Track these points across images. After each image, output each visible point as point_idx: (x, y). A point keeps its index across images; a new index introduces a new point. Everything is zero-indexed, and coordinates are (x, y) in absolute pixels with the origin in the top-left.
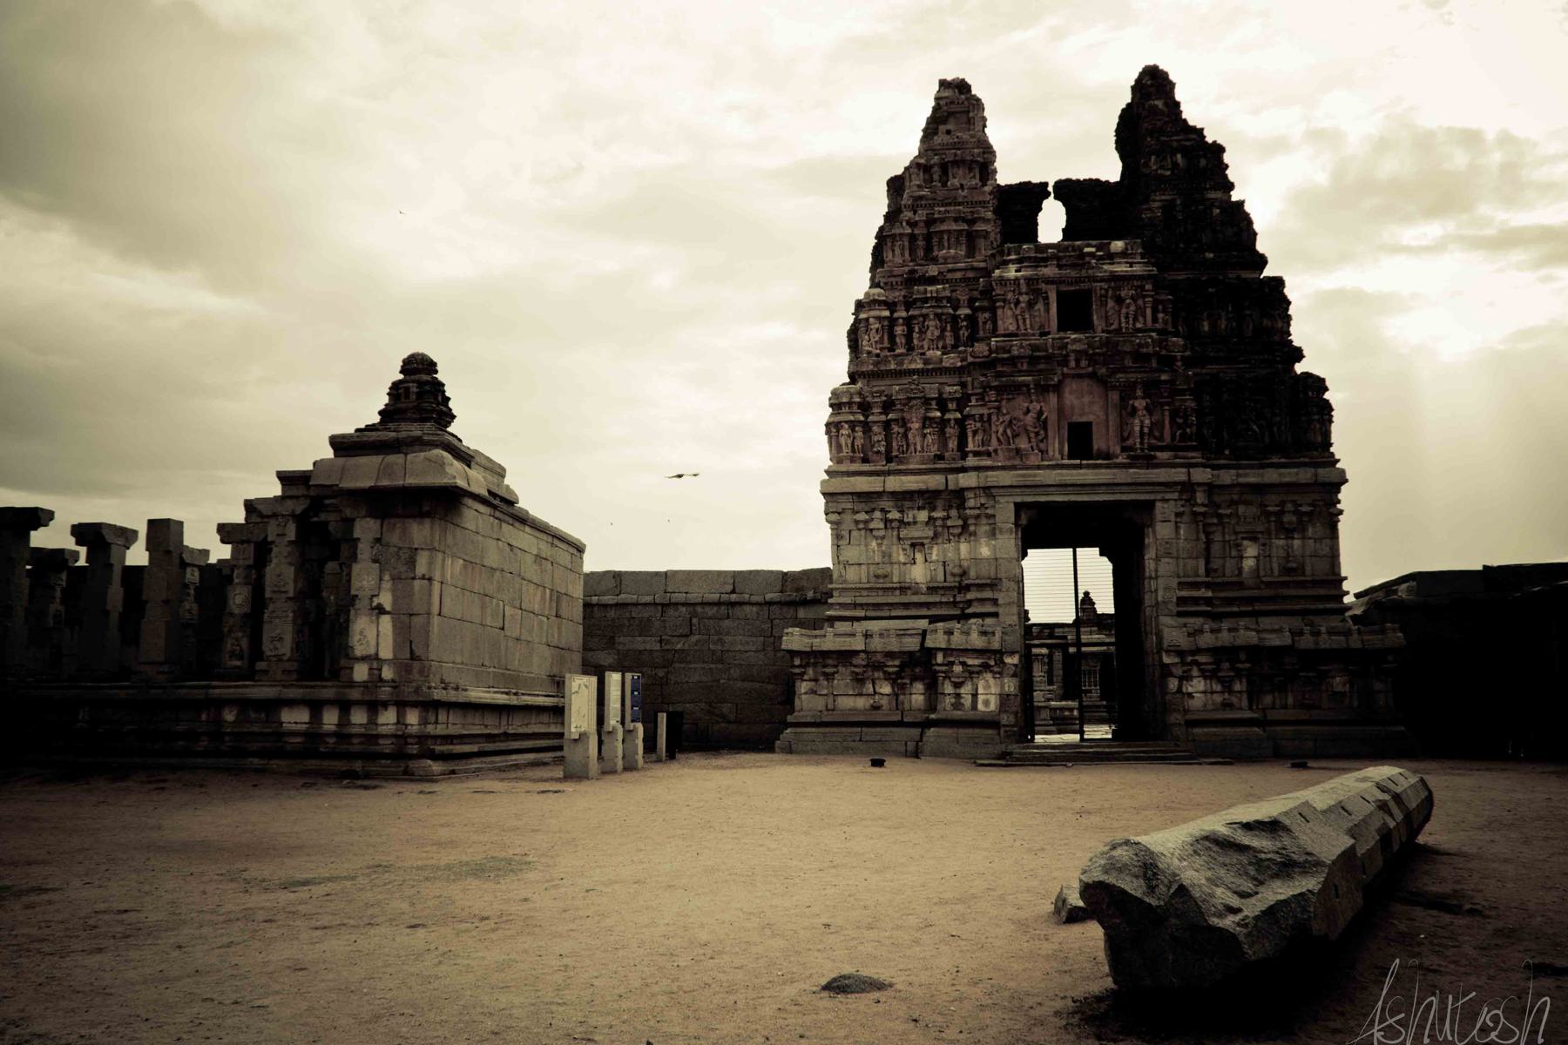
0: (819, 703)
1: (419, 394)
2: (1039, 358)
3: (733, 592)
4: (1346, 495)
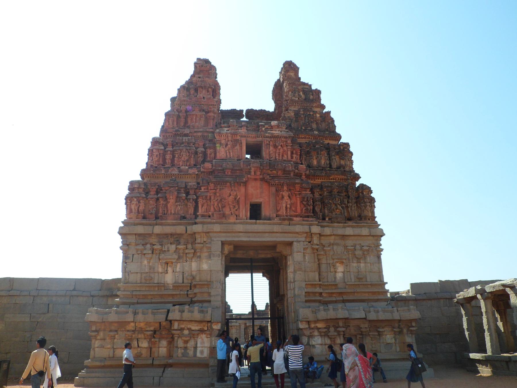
0: (105, 353)
2: (237, 170)
3: (74, 290)
4: (384, 242)
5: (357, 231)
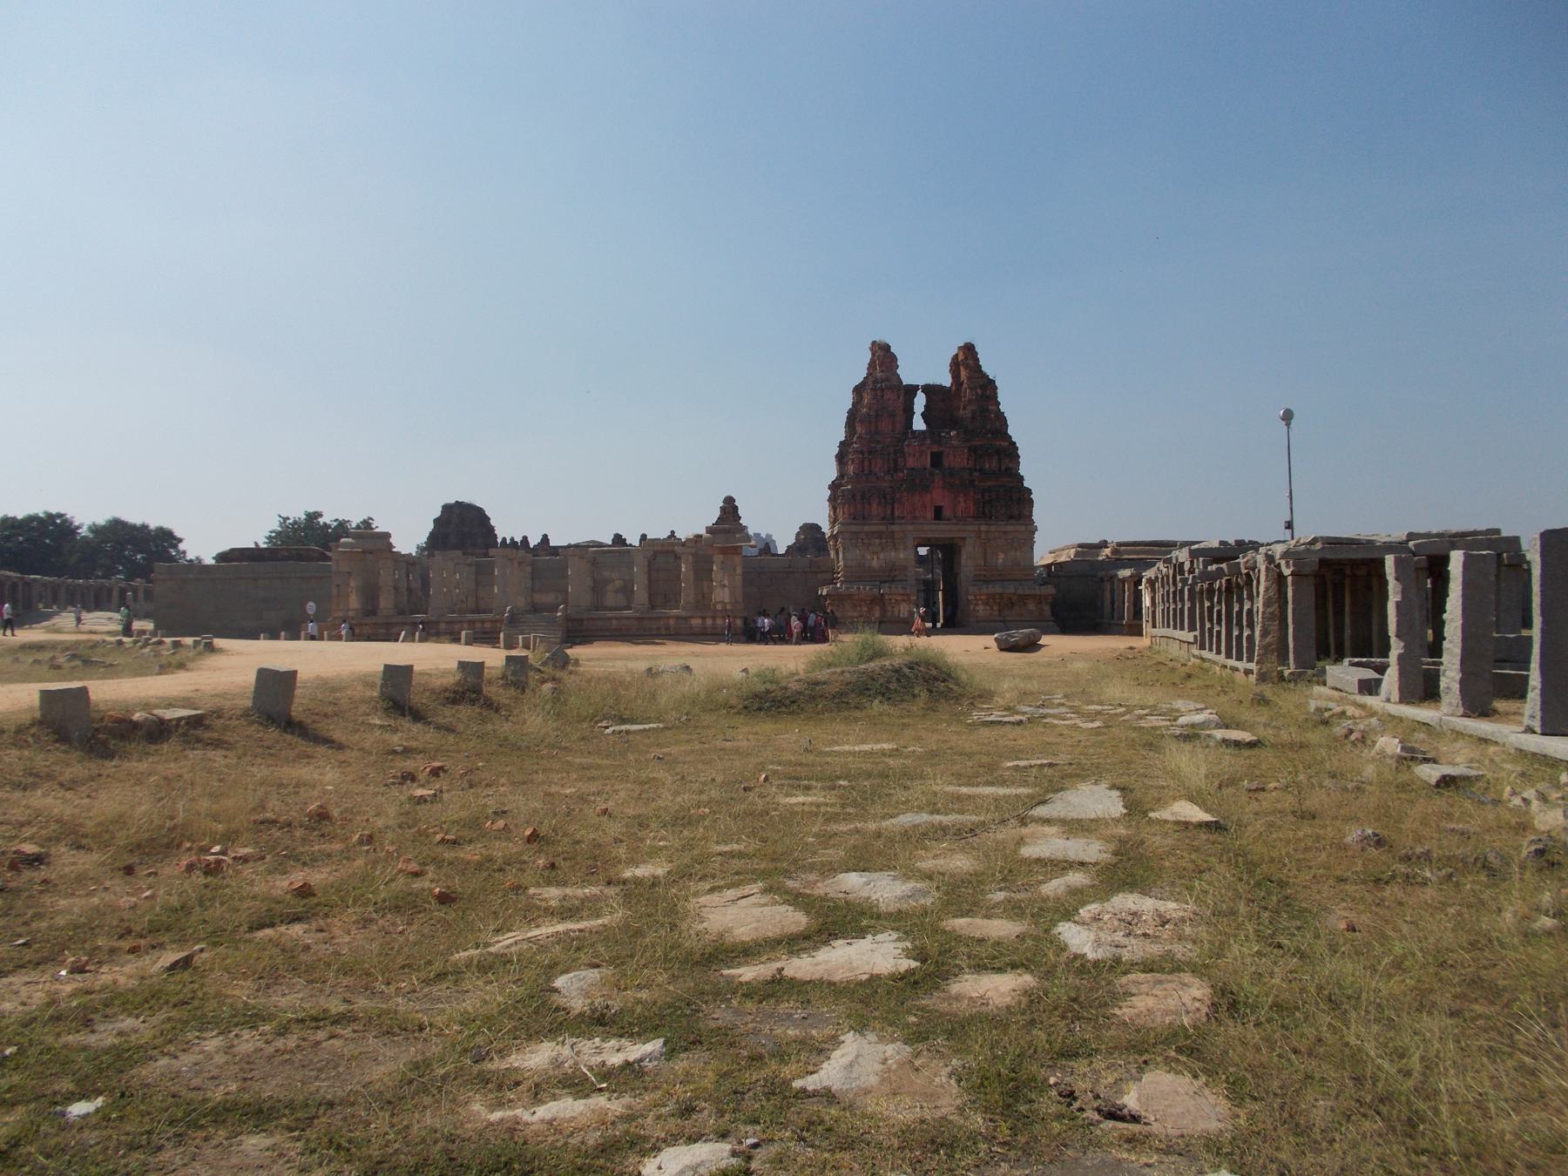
1: (730, 509)
5: (1018, 528)
